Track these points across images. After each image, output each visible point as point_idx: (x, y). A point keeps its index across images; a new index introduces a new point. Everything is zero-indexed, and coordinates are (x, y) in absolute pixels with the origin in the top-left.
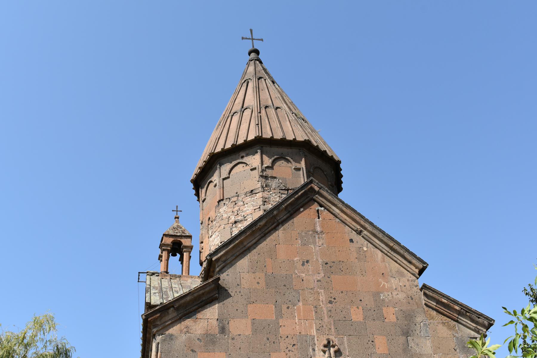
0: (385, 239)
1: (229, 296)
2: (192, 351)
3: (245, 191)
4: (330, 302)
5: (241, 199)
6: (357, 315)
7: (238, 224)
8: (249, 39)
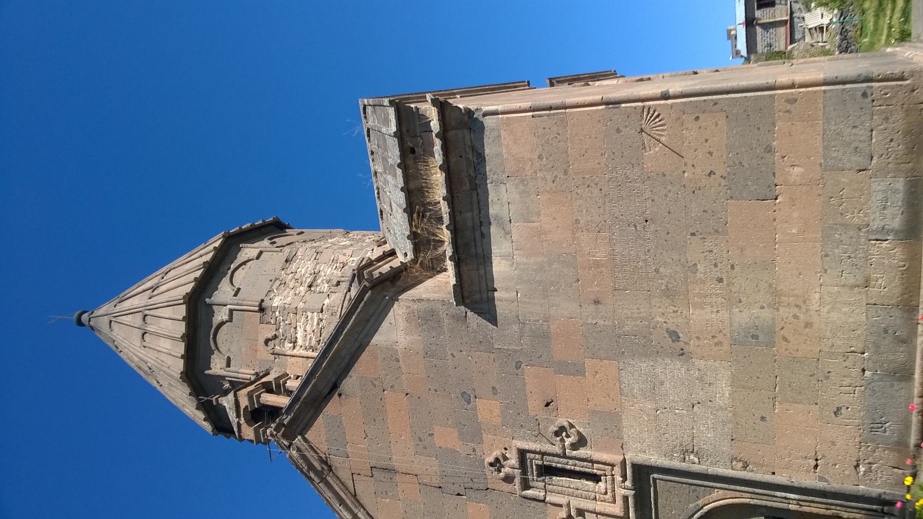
3: (279, 268)
5: (285, 275)
7: (315, 284)
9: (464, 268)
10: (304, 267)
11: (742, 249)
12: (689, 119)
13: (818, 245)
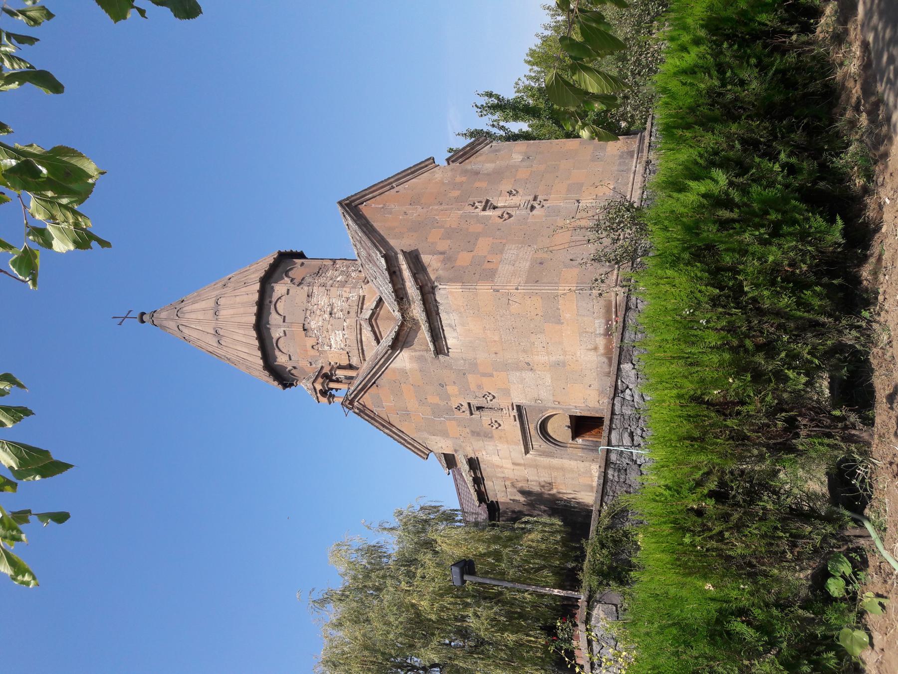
0: (404, 174)
1: (417, 250)
2: (452, 268)
3: (305, 302)
4: (441, 204)
6: (456, 193)
7: (333, 312)
8: (123, 320)
9: (436, 343)
10: (321, 299)
11: (551, 338)
12: (527, 297)
13: (578, 338)
